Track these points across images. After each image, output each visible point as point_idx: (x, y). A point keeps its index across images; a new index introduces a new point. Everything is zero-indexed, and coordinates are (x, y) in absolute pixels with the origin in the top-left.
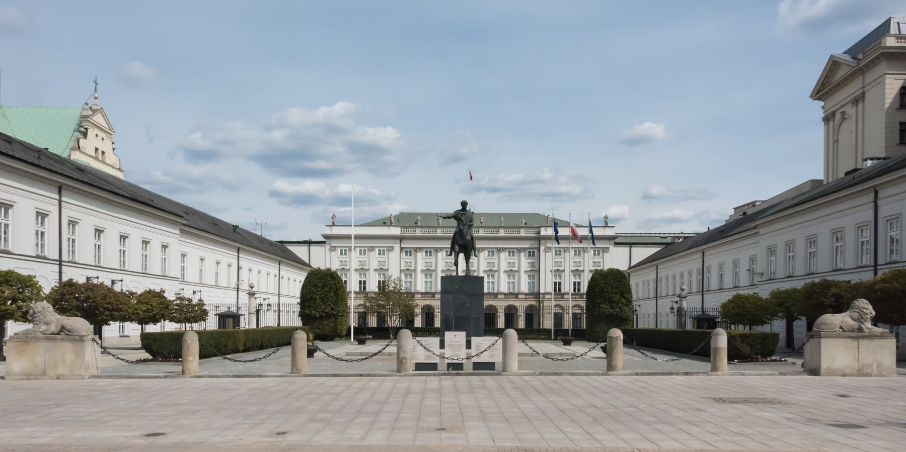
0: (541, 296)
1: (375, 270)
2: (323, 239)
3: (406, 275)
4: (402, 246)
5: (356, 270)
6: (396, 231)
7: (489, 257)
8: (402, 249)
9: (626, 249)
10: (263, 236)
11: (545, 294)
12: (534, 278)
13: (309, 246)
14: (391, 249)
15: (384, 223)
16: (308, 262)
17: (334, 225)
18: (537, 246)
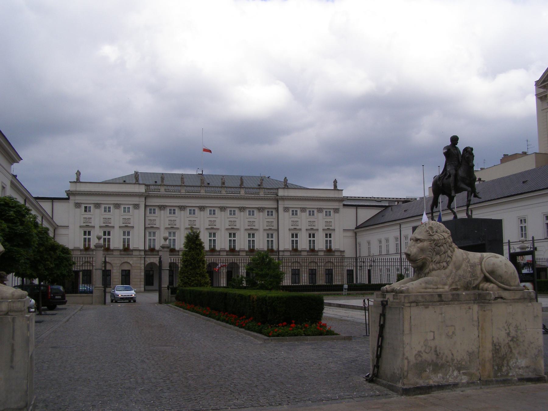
0: (281, 254)
1: (120, 227)
2: (65, 196)
3: (150, 233)
4: (147, 204)
5: (101, 227)
6: (142, 189)
7: (231, 216)
8: (146, 206)
9: (353, 211)
11: (283, 251)
12: (272, 237)
13: (53, 202)
14: (136, 206)
15: (124, 181)
18: (276, 206)
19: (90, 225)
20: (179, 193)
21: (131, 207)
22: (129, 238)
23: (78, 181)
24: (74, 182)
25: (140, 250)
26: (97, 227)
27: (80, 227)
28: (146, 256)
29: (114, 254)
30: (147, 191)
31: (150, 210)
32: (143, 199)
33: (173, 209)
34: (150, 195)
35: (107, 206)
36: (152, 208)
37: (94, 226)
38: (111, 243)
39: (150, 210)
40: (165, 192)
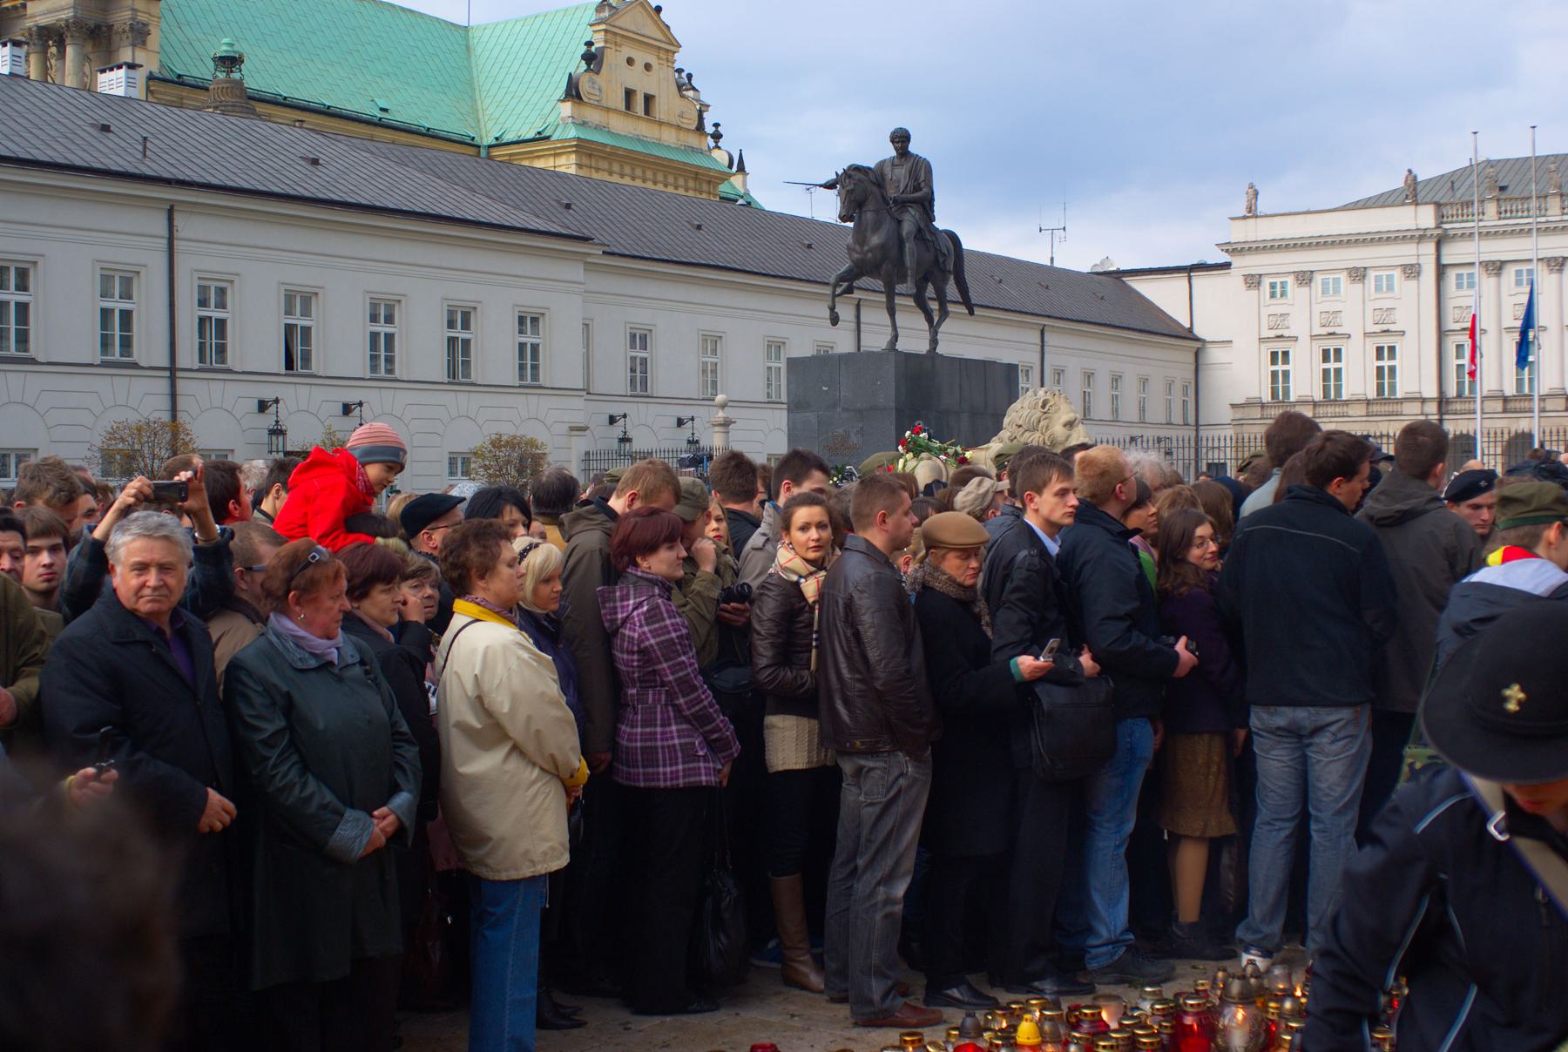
4: (1445, 261)
5: (1314, 337)
8: (1441, 269)
10: (1057, 264)
13: (1190, 279)
14: (1412, 271)
17: (1252, 213)
19: (1286, 333)
20: (1543, 219)
21: (1397, 273)
22: (1288, 371)
23: (1252, 213)
24: (1245, 218)
25: (1424, 401)
26: (1357, 336)
27: (1261, 340)
28: (1445, 417)
29: (1350, 413)
30: (1446, 223)
31: (1457, 279)
32: (1430, 248)
33: (1468, 274)
34: (1452, 233)
35: (1332, 276)
36: (1465, 271)
37: (1404, 332)
38: (1344, 382)
39: (1459, 276)
40: (1500, 219)
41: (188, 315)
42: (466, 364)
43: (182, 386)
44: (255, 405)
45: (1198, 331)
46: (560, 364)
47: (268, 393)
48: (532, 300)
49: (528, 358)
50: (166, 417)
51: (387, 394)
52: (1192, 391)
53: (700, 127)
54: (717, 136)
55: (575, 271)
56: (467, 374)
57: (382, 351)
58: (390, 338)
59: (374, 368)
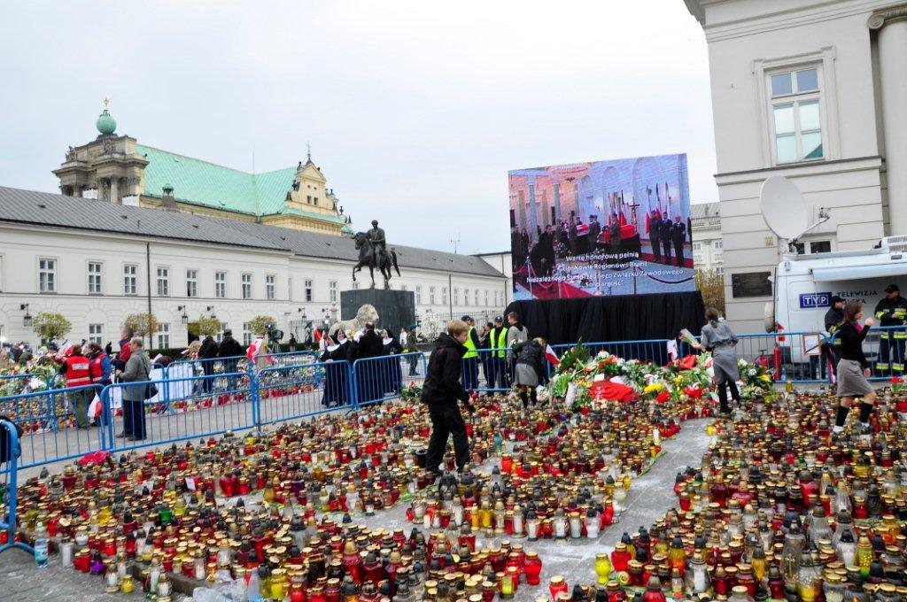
16: (501, 270)
41: (154, 278)
42: (249, 293)
43: (152, 302)
44: (177, 308)
45: (505, 274)
46: (281, 290)
47: (182, 304)
48: (271, 271)
49: (270, 290)
50: (147, 313)
51: (223, 304)
52: (504, 294)
53: (335, 208)
54: (341, 211)
55: (285, 261)
56: (249, 296)
57: (220, 290)
58: (223, 285)
59: (218, 295)
